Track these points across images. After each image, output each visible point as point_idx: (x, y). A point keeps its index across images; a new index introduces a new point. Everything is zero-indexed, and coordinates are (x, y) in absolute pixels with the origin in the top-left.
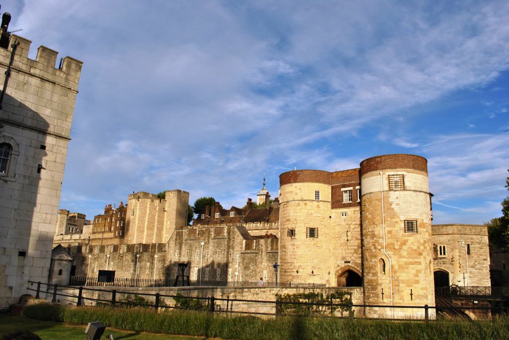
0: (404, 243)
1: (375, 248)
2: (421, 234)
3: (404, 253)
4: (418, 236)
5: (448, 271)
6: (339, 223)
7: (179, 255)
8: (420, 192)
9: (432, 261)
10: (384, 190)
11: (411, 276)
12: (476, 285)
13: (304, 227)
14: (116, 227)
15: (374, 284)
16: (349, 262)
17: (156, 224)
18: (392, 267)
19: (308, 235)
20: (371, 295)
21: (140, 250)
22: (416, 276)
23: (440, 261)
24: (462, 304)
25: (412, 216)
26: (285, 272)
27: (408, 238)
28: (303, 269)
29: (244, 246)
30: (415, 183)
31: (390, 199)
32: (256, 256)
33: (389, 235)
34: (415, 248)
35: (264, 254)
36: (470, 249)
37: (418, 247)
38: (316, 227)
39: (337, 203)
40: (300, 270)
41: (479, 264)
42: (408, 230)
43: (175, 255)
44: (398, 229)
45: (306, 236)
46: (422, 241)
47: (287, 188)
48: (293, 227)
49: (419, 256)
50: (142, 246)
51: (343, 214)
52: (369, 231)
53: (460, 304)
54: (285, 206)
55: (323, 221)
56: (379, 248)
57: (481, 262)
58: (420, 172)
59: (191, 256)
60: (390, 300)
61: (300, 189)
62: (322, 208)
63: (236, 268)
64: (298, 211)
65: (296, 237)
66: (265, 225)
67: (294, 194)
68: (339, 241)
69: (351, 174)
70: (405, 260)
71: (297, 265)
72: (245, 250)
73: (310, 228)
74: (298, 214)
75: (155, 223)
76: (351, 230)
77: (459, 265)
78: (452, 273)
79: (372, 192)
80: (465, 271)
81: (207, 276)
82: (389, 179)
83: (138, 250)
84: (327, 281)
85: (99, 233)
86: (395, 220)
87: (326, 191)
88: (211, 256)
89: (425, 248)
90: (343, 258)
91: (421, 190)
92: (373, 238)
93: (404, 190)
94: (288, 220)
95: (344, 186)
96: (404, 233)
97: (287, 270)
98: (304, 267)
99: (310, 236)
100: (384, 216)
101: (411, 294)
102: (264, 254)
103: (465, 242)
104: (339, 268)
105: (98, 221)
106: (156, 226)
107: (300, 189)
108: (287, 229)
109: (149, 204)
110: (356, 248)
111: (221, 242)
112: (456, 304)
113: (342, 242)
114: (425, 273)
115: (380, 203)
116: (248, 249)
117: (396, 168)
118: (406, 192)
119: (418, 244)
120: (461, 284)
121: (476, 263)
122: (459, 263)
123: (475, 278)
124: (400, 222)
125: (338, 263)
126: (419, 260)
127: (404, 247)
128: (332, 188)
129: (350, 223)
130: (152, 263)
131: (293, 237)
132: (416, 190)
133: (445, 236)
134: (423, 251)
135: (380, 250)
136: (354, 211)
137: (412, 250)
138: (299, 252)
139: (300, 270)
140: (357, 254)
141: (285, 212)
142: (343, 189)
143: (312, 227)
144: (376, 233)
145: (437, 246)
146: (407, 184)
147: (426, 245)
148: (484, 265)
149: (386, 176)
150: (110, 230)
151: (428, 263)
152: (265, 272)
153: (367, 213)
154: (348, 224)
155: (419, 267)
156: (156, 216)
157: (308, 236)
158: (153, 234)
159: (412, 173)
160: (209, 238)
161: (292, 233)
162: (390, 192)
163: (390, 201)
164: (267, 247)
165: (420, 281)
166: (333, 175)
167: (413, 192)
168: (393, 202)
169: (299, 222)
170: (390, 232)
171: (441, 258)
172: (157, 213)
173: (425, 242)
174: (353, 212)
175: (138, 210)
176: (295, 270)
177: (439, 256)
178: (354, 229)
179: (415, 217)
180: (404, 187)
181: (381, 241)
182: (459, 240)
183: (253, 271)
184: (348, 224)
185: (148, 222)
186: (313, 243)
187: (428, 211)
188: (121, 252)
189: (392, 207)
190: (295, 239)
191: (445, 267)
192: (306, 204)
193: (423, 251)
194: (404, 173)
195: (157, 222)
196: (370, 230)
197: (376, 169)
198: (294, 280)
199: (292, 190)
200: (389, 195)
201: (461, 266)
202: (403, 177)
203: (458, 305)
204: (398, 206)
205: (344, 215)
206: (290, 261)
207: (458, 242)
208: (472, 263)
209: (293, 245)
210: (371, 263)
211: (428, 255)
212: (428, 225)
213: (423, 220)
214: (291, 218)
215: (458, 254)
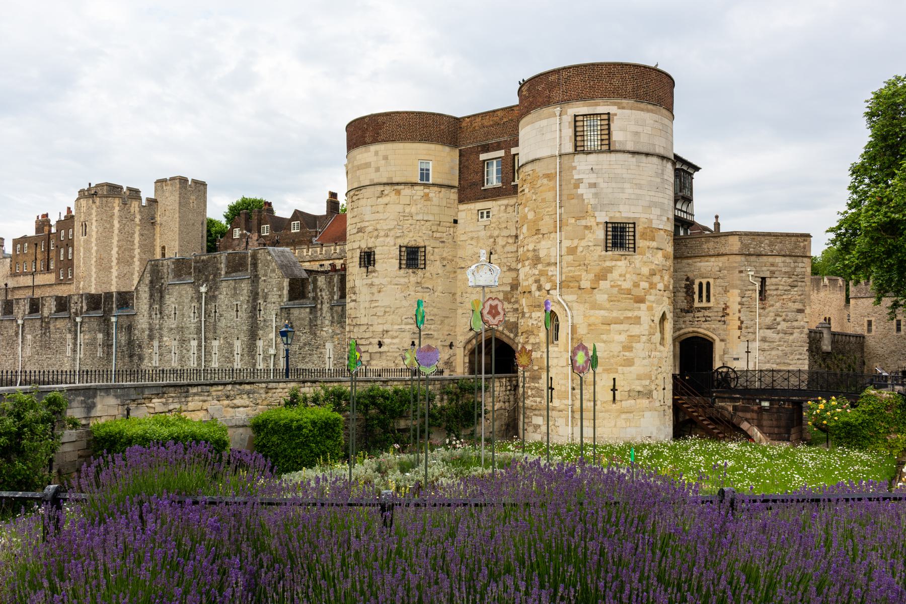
0: (602, 276)
1: (540, 288)
2: (643, 254)
3: (601, 297)
4: (637, 259)
5: (714, 337)
7: (159, 316)
8: (647, 154)
9: (669, 316)
10: (563, 152)
11: (616, 348)
12: (775, 367)
13: (395, 245)
14: (58, 261)
15: (536, 368)
17: (137, 251)
18: (574, 328)
19: (404, 262)
20: (530, 393)
21: (82, 307)
22: (628, 348)
23: (697, 314)
24: (735, 408)
25: (623, 214)
27: (614, 263)
28: (393, 338)
29: (285, 292)
30: (637, 133)
31: (574, 172)
33: (570, 258)
34: (627, 285)
35: (326, 307)
36: (767, 288)
37: (636, 285)
38: (422, 244)
39: (470, 188)
40: (386, 341)
41: (784, 320)
42: (615, 245)
44: (590, 244)
45: (397, 266)
46: (645, 271)
47: (358, 157)
48: (370, 245)
49: (636, 305)
50: (87, 298)
51: (482, 213)
52: (528, 251)
53: (731, 409)
54: (355, 198)
55: (437, 231)
56: (548, 286)
57: (791, 315)
58: (650, 107)
60: (565, 402)
61: (386, 158)
62: (435, 201)
63: (272, 340)
64: (380, 209)
65: (378, 266)
67: (372, 170)
69: (501, 119)
70: (603, 313)
71: (380, 328)
72: (290, 300)
73: (406, 247)
74: (381, 216)
75: (134, 249)
76: (498, 248)
77: (739, 323)
78: (722, 340)
79: (537, 157)
80: (751, 336)
81: (215, 358)
82: (575, 127)
83: (79, 308)
84: (446, 363)
85: (25, 274)
86: (583, 222)
89: (652, 286)
91: (651, 151)
92: (535, 265)
93: (610, 151)
95: (486, 149)
96: (604, 253)
97: (359, 342)
98: (395, 334)
99: (408, 266)
100: (560, 214)
101: (614, 390)
103: (757, 272)
105: (22, 248)
106: (137, 256)
107: (386, 158)
108: (358, 251)
109: (117, 208)
110: (508, 289)
112: (722, 408)
114: (650, 340)
115: (551, 184)
116: (296, 299)
117: (592, 98)
118: (613, 156)
119: (635, 278)
120: (740, 365)
121: (779, 319)
122: (739, 318)
123: (774, 353)
124: (595, 227)
126: (636, 313)
127: (603, 284)
129: (496, 233)
130: (108, 334)
131: (370, 268)
132: (636, 150)
133: (713, 259)
134: (647, 292)
135: (548, 291)
136: (507, 206)
137: (621, 291)
139: (385, 340)
140: (510, 302)
142: (483, 157)
143: (412, 244)
144: (542, 254)
145: (693, 283)
146: (617, 136)
147: (656, 279)
148: (795, 324)
149: (568, 119)
150: (48, 269)
151: (657, 320)
152: (329, 346)
153: (527, 209)
154: (491, 237)
155: (635, 330)
156: (137, 236)
157: (403, 266)
158: (132, 274)
159: (648, 111)
161: (368, 259)
162: (577, 156)
163: (576, 177)
164: (332, 293)
165: (636, 360)
166: (464, 124)
167: (630, 156)
168: (580, 181)
169: (382, 233)
170: (572, 251)
171: (699, 309)
172: (138, 228)
173: (653, 273)
174: (503, 208)
175: (94, 221)
176: (375, 341)
177: (697, 304)
178: (504, 247)
179: (632, 215)
180: (609, 144)
181: (551, 271)
182: (743, 269)
184: (491, 237)
185: (119, 247)
186: (413, 279)
187: (666, 202)
188: (46, 313)
189: (580, 191)
190: (374, 271)
191: (708, 329)
192: (398, 193)
193: (647, 292)
194: (612, 109)
195: (140, 247)
196: (531, 247)
198: (373, 362)
199: (368, 161)
200: (574, 164)
201: (744, 326)
202: (609, 120)
203: (727, 410)
204: (593, 190)
205: (485, 215)
206: (364, 320)
207: (741, 272)
208: (768, 320)
209: (372, 284)
210: (530, 322)
211: (659, 302)
212: (662, 232)
213: (651, 221)
214: (367, 224)
215: (739, 299)
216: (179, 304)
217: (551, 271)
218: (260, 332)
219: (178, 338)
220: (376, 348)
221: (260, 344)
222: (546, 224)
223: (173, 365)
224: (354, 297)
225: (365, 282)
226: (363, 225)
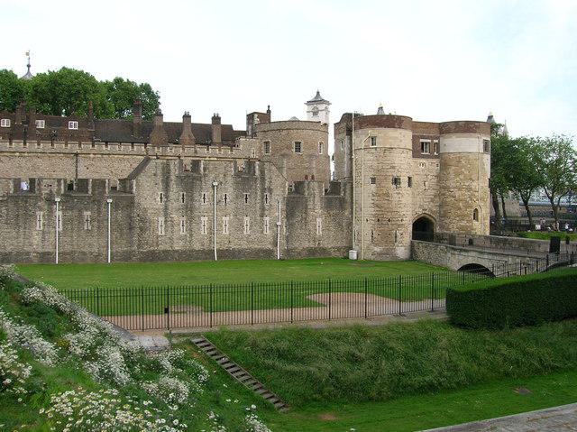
7: (164, 199)
35: (317, 198)
59: (192, 200)
87: (404, 138)
90: (420, 206)
94: (394, 167)
138: (404, 201)
142: (422, 140)
149: (481, 141)
152: (319, 220)
161: (396, 181)
164: (321, 192)
181: (476, 194)
217: (476, 194)
218: (266, 212)
222: (474, 177)
223: (181, 233)
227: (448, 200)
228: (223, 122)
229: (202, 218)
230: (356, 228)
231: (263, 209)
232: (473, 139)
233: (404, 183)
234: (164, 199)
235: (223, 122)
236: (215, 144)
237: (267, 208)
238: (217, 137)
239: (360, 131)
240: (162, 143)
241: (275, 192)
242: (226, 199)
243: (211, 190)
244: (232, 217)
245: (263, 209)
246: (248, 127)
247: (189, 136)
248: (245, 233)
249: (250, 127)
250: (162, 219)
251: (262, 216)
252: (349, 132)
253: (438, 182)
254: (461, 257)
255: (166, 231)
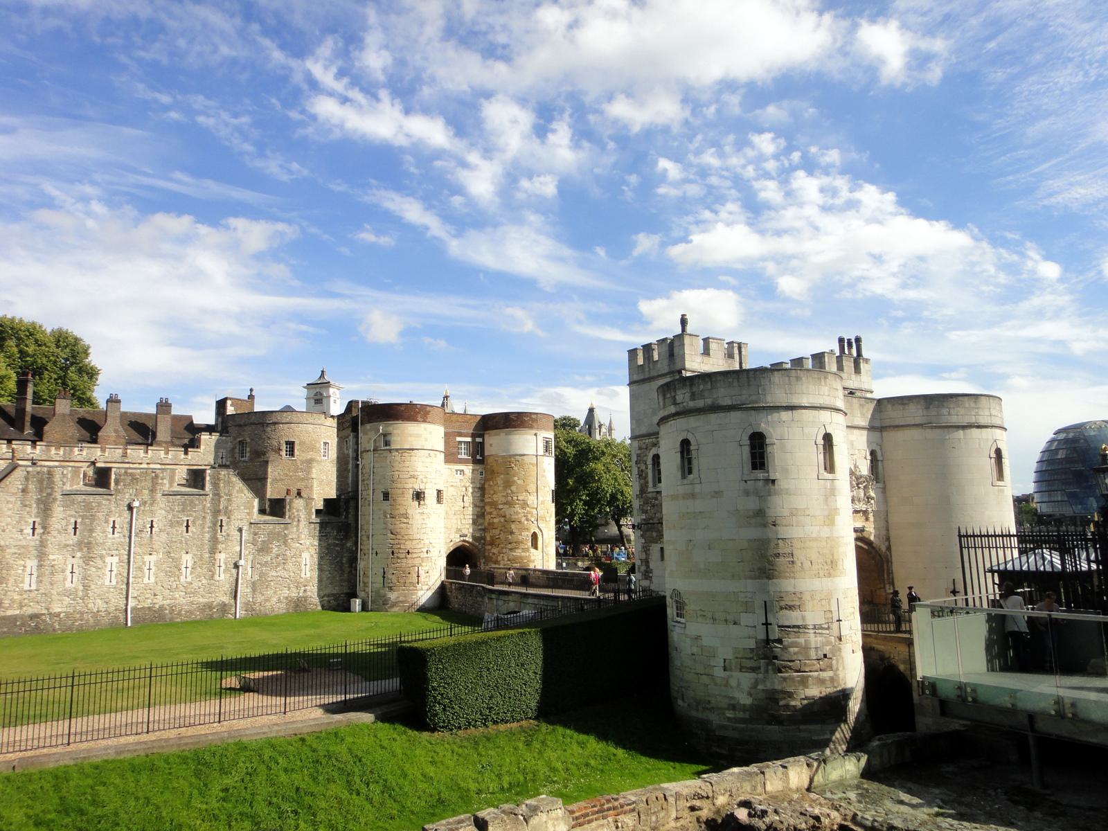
1: (527, 520)
6: (455, 484)
16: (466, 536)
26: (408, 552)
32: (286, 529)
40: (431, 549)
43: (21, 531)
59: (91, 531)
66: (49, 451)
68: (453, 508)
88: (161, 531)
90: (458, 530)
94: (413, 476)
95: (461, 435)
102: (303, 524)
104: (452, 543)
107: (431, 433)
111: (192, 502)
113: (457, 508)
125: (452, 537)
128: (446, 434)
131: (422, 502)
141: (407, 464)
142: (458, 439)
153: (516, 478)
160: (153, 491)
161: (419, 496)
164: (309, 514)
176: (425, 550)
181: (534, 512)
183: (278, 556)
184: (464, 486)
190: (425, 504)
197: (531, 427)
198: (423, 564)
214: (419, 474)
216: (83, 517)
218: (220, 546)
219: (79, 554)
220: (426, 555)
221: (221, 557)
223: (68, 584)
224: (405, 521)
225: (418, 511)
226: (416, 473)
227: (496, 521)
228: (176, 410)
229: (108, 560)
230: (361, 565)
231: (214, 541)
232: (529, 437)
233: (430, 497)
234: (39, 530)
235: (176, 410)
236: (159, 444)
237: (220, 538)
238: (163, 433)
239: (368, 426)
240: (66, 441)
241: (236, 515)
242: (152, 527)
243: (127, 514)
244: (161, 556)
245: (214, 541)
246: (217, 420)
247: (116, 431)
248: (183, 579)
249: (220, 419)
250: (32, 564)
251: (213, 551)
252: (355, 429)
253: (483, 495)
254: (500, 603)
255: (39, 582)
